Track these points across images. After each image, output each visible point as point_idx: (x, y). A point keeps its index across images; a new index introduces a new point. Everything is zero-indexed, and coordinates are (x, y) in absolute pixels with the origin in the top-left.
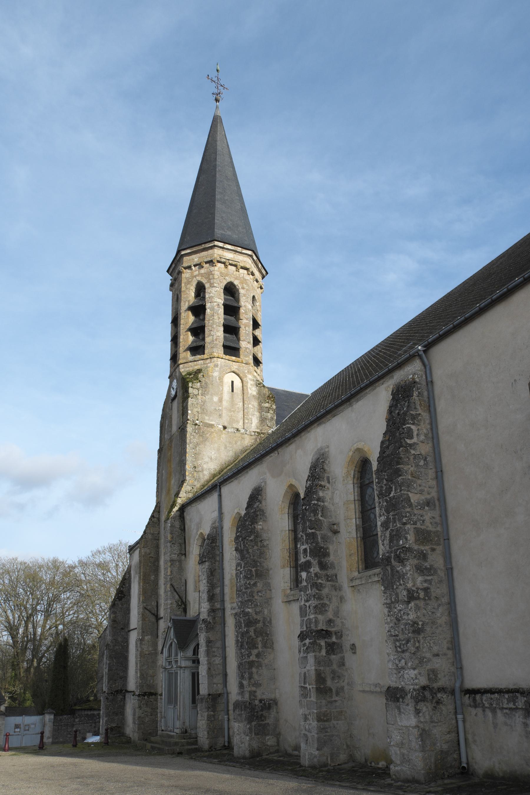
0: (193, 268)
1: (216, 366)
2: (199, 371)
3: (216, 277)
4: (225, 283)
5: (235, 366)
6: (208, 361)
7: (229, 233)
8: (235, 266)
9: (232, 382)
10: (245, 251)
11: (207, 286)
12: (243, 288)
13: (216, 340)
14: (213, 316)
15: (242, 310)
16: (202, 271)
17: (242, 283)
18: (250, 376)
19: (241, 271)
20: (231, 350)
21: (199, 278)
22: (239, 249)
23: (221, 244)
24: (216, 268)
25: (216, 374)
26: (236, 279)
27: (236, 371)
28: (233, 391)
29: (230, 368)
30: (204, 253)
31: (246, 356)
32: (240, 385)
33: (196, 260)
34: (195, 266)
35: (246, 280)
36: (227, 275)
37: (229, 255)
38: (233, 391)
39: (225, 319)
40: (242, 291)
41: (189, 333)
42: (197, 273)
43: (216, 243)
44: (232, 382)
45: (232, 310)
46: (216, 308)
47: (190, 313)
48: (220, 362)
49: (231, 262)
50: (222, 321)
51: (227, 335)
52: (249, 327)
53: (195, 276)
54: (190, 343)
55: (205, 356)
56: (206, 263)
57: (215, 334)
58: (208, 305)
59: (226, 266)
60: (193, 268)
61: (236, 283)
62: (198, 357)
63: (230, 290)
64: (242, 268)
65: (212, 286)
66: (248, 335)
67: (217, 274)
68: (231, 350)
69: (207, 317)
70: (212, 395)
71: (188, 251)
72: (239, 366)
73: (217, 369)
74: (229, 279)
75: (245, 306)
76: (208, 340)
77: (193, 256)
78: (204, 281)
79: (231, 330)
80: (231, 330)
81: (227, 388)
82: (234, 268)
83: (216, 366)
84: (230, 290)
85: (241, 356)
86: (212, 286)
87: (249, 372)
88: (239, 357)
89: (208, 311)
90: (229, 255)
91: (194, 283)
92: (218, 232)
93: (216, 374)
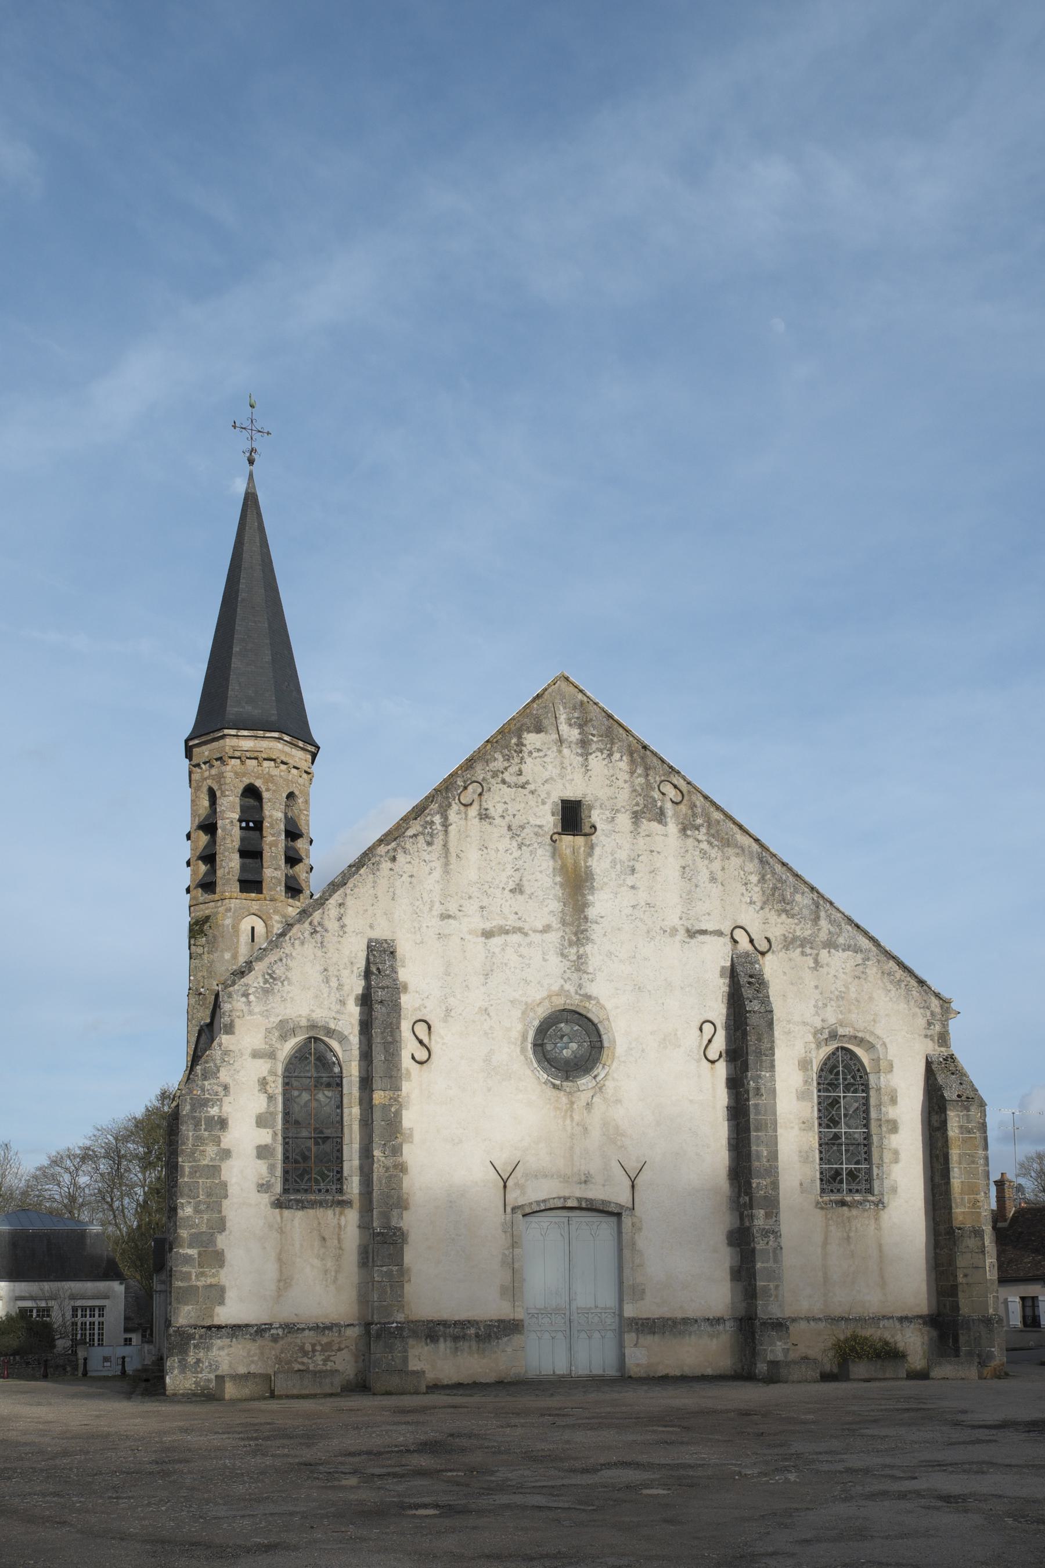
0: (203, 766)
1: (229, 910)
2: (207, 919)
3: (228, 781)
4: (242, 786)
5: (255, 906)
6: (220, 903)
7: (249, 708)
8: (256, 758)
9: (253, 928)
10: (268, 734)
11: (218, 794)
12: (268, 790)
13: (228, 873)
14: (224, 839)
15: (266, 824)
16: (214, 771)
17: (266, 782)
18: (277, 918)
19: (266, 764)
20: (251, 884)
21: (209, 782)
22: (260, 733)
23: (233, 732)
24: (228, 768)
25: (228, 922)
26: (257, 778)
27: (257, 912)
28: (253, 940)
29: (248, 910)
30: (215, 744)
31: (271, 889)
32: (264, 930)
33: (206, 753)
34: (205, 763)
35: (272, 776)
36: (244, 775)
37: (247, 744)
38: (253, 940)
39: (242, 840)
40: (266, 795)
41: (200, 862)
42: (207, 774)
43: (226, 731)
44: (253, 928)
45: (253, 822)
46: (228, 827)
47: (201, 833)
48: (233, 904)
49: (248, 754)
50: (237, 844)
51: (248, 861)
52: (276, 846)
53: (205, 779)
54: (201, 876)
55: (216, 897)
56: (217, 760)
57: (230, 863)
58: (220, 823)
59: (243, 763)
60: (203, 766)
61: (258, 783)
62: (211, 897)
63: (252, 793)
64: (265, 759)
65: (223, 795)
66: (275, 858)
67: (229, 775)
68: (251, 884)
69: (218, 840)
70: (222, 951)
71: (196, 742)
72: (262, 905)
73: (229, 914)
74: (247, 781)
75: (271, 816)
76: (219, 873)
77: (204, 748)
78: (215, 788)
79: (251, 853)
80: (251, 853)
81: (244, 937)
82: (254, 762)
83: (229, 910)
84: (252, 793)
85: (264, 892)
86: (223, 795)
87: (276, 912)
88: (261, 893)
89: (219, 831)
90: (247, 744)
91: (205, 789)
92: (232, 710)
93: (228, 922)
